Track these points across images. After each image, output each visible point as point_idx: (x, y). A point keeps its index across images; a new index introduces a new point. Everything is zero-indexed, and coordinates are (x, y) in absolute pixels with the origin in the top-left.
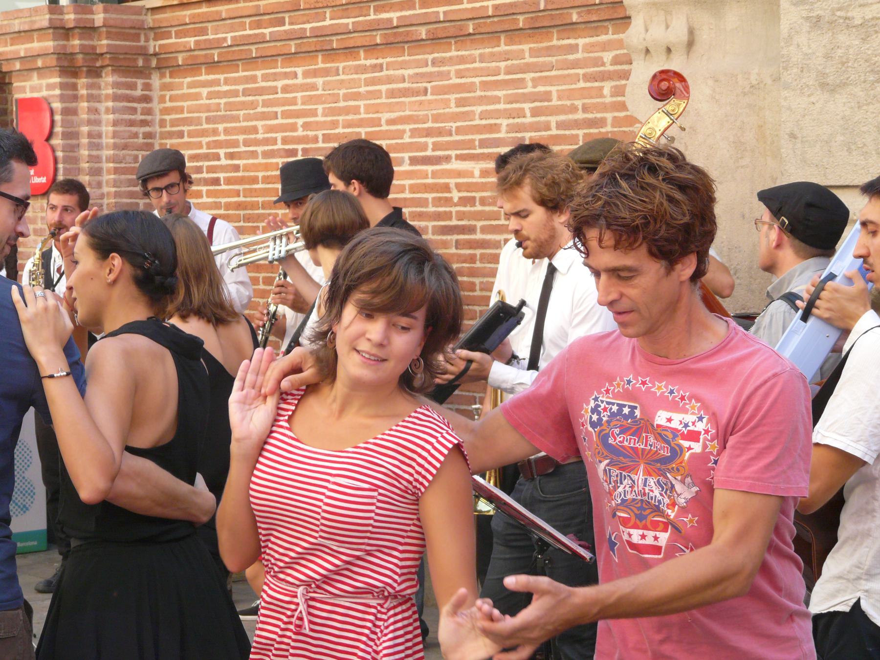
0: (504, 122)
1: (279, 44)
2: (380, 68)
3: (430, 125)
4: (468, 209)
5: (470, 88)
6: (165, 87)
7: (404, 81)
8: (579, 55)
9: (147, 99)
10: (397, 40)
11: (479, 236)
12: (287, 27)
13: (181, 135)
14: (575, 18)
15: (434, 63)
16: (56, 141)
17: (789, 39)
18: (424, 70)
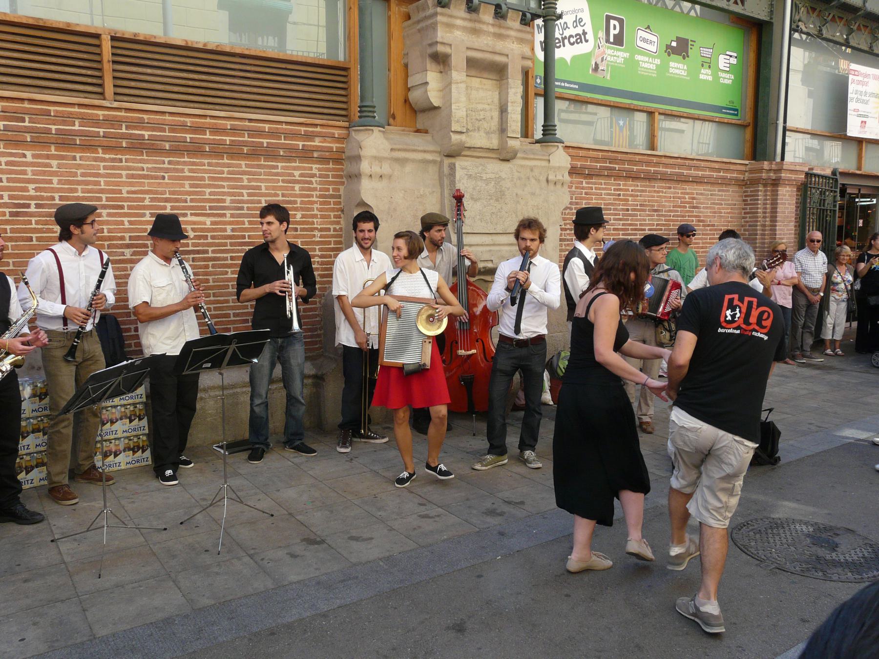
0: (228, 199)
1: (10, 133)
2: (121, 160)
3: (167, 196)
4: (202, 241)
5: (203, 179)
7: (143, 170)
8: (279, 171)
10: (138, 146)
11: (210, 255)
12: (27, 124)
14: (282, 153)
15: (170, 163)
17: (460, 181)
18: (162, 166)
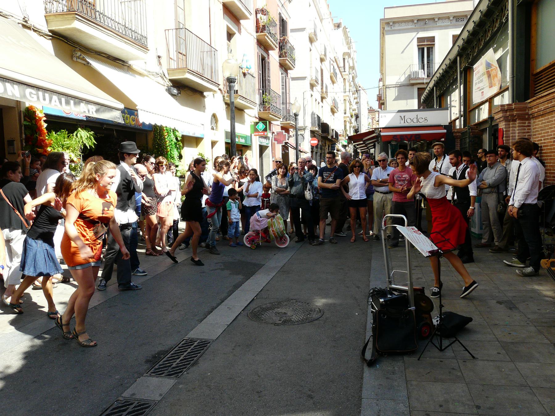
6: (534, 122)
9: (529, 126)
13: (536, 135)
16: (504, 139)
